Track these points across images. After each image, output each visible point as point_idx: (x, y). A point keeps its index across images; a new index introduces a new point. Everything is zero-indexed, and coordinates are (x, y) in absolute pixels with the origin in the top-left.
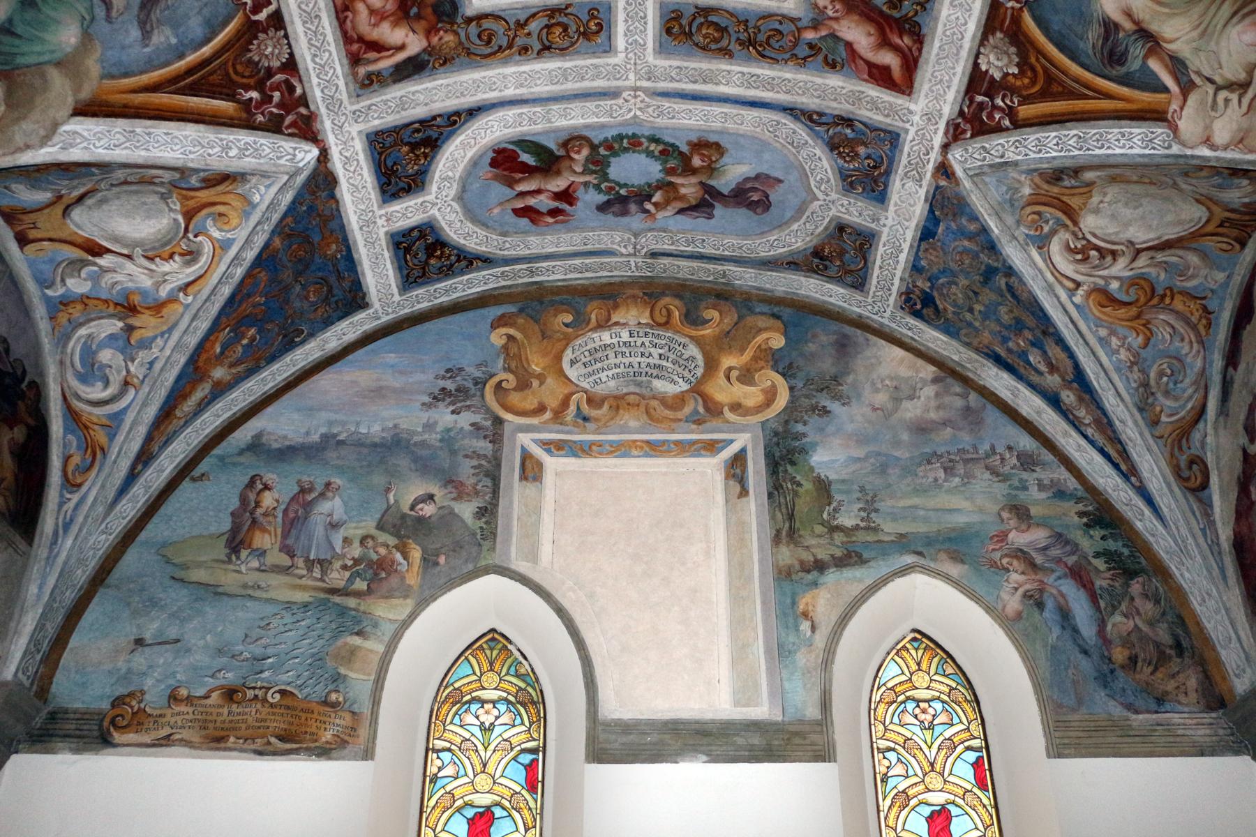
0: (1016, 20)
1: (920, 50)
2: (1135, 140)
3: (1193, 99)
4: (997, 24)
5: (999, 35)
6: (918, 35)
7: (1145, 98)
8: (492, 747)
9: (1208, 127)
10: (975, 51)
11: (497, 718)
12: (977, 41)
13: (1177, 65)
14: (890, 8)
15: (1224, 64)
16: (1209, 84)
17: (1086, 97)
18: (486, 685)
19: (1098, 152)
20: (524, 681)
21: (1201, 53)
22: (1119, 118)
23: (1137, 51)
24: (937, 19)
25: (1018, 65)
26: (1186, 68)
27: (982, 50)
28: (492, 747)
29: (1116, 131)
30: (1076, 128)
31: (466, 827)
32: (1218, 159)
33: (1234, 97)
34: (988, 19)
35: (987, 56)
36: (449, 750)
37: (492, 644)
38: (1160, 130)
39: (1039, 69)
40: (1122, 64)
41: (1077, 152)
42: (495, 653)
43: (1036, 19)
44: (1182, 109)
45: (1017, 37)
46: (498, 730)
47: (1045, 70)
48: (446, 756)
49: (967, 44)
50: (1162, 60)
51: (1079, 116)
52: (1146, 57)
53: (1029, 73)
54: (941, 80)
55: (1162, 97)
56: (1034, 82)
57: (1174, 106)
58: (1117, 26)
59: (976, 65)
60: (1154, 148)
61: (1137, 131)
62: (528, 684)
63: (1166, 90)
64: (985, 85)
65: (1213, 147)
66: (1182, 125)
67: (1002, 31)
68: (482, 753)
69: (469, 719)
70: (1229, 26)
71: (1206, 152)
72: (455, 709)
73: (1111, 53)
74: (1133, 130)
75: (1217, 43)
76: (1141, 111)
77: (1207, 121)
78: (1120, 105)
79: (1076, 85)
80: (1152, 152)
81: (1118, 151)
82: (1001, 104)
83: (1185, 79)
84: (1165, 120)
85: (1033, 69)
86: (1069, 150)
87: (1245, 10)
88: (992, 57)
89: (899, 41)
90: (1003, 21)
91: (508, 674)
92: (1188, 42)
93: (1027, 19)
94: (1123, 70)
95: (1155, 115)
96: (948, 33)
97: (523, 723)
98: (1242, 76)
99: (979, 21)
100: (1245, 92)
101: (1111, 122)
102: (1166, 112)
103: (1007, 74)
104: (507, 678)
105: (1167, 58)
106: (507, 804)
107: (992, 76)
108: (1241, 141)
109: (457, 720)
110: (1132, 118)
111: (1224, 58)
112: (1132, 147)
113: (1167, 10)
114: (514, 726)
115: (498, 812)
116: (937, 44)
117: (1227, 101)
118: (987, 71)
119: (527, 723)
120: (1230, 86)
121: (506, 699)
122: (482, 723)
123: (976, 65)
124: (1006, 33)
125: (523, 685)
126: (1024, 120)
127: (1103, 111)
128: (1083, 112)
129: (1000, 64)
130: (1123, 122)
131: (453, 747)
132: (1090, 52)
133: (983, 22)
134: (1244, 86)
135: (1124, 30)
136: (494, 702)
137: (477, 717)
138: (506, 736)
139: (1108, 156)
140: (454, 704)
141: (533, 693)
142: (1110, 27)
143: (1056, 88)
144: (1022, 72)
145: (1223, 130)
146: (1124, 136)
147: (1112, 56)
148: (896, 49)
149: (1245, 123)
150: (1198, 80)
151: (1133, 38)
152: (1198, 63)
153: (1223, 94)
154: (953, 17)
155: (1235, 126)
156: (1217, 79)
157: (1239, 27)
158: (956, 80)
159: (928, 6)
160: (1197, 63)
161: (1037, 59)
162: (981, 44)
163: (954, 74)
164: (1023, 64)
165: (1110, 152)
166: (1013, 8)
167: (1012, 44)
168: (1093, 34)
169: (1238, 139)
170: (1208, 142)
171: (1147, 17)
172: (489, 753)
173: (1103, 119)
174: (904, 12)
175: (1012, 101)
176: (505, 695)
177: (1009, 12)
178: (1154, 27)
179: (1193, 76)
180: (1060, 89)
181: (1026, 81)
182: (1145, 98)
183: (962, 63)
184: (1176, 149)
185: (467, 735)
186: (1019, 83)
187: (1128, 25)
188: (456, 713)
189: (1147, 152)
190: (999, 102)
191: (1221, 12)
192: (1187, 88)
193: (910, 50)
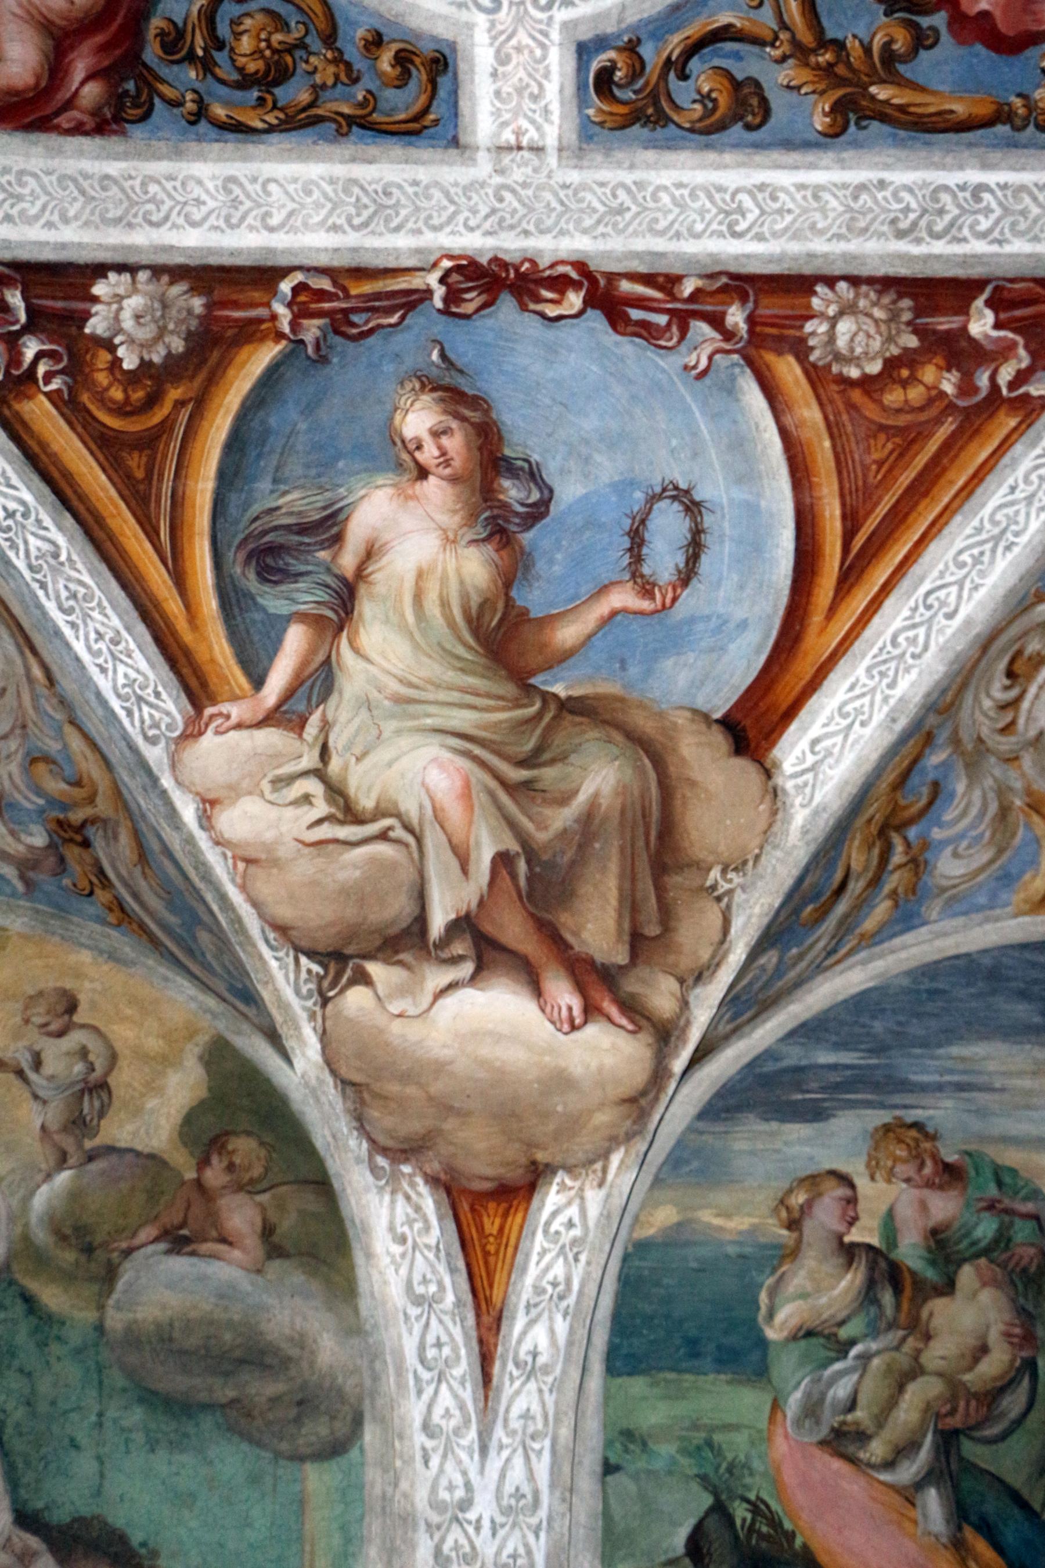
0: (252, 332)
1: (78, 130)
2: (121, 669)
3: (271, 737)
4: (220, 293)
5: (197, 303)
6: (118, 119)
7: (217, 648)
9: (235, 792)
10: (132, 259)
12: (162, 259)
13: (318, 681)
14: (162, 34)
15: (367, 762)
16: (316, 752)
17: (151, 533)
19: (51, 607)
21: (364, 714)
22: (145, 616)
23: (307, 596)
24: (178, 154)
25: (145, 365)
26: (323, 699)
27: (143, 276)
29: (116, 622)
30: (71, 540)
32: (190, 840)
33: (321, 808)
34: (222, 269)
35: (135, 290)
38: (172, 707)
39: (158, 416)
40: (263, 578)
41: (20, 564)
43: (270, 380)
44: (239, 726)
45: (211, 347)
47: (166, 427)
49: (142, 240)
50: (312, 651)
51: (100, 535)
52: (302, 617)
53: (138, 395)
54: (19, 198)
55: (240, 679)
56: (122, 410)
57: (236, 711)
58: (338, 539)
59: (100, 270)
60: (130, 713)
61: (143, 665)
63: (258, 682)
64: (60, 304)
65: (206, 820)
66: (208, 740)
67: (209, 306)
70: (439, 738)
71: (188, 812)
73: (273, 550)
74: (137, 655)
75: (398, 732)
76: (187, 653)
77: (245, 784)
78: (174, 606)
79: (166, 503)
80: (122, 714)
81: (79, 647)
82: (29, 354)
83: (301, 707)
84: (198, 706)
85: (153, 400)
86: (14, 546)
87: (477, 751)
88: (134, 303)
89: (79, 69)
90: (236, 305)
92: (372, 681)
93: (261, 358)
94: (251, 582)
95: (193, 683)
96: (153, 188)
98: (367, 803)
99: (210, 251)
100: (342, 823)
101: (125, 603)
102: (213, 701)
103: (112, 348)
105: (320, 657)
107: (87, 315)
108: (249, 861)
110: (159, 640)
111: (381, 755)
112: (103, 670)
113: (410, 618)
116: (114, 168)
117: (306, 799)
118: (95, 299)
120: (336, 791)
123: (100, 270)
124: (207, 319)
126: (17, 415)
127: (140, 578)
128: (111, 537)
129: (128, 323)
130: (141, 628)
132: (256, 509)
133: (213, 261)
134: (348, 812)
135: (334, 557)
139: (58, 633)
142: (329, 527)
143: (136, 463)
144: (132, 378)
145: (247, 819)
146: (115, 642)
147: (270, 556)
148: (56, 67)
149: (286, 850)
150: (312, 729)
151: (329, 580)
152: (344, 715)
153: (313, 786)
154: (197, 191)
155: (269, 836)
156: (335, 765)
157: (447, 755)
158: (36, 233)
159: (203, 126)
160: (343, 716)
161: (180, 404)
162: (157, 271)
163: (50, 225)
164: (153, 378)
165: (68, 632)
166: (274, 317)
167: (189, 337)
168: (297, 502)
169: (252, 854)
170: (209, 806)
171: (380, 589)
173: (124, 586)
174: (164, 71)
175: (48, 377)
177: (261, 312)
178: (367, 608)
179: (315, 719)
180: (140, 474)
181: (117, 394)
182: (217, 648)
183: (87, 237)
184: (155, 755)
186: (102, 378)
187: (348, 561)
189: (115, 704)
190: (31, 348)
191: (456, 712)
192: (286, 716)
193: (70, 104)
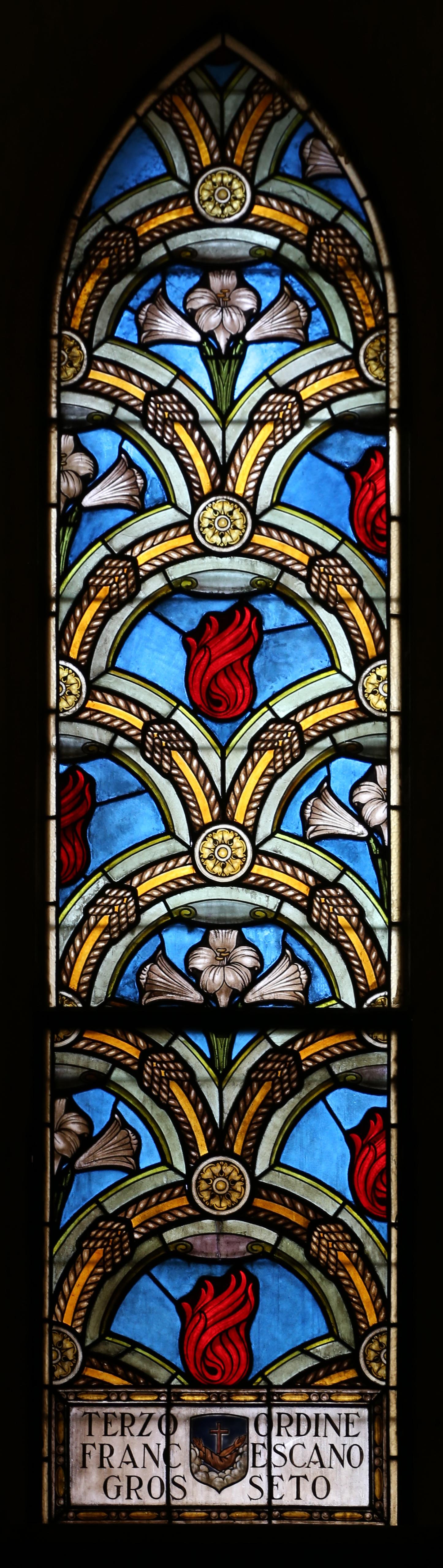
8: (242, 411)
11: (252, 318)
18: (210, 210)
20: (332, 198)
28: (242, 411)
31: (181, 658)
36: (109, 423)
37: (221, 74)
42: (232, 103)
46: (255, 361)
48: (105, 443)
62: (344, 208)
68: (214, 432)
69: (170, 324)
72: (117, 290)
91: (277, 173)
97: (333, 336)
104: (277, 186)
106: (299, 588)
109: (126, 328)
114: (305, 344)
115: (273, 614)
119: (346, 335)
121: (274, 256)
122: (208, 336)
125: (326, 210)
131: (123, 414)
136: (241, 267)
137: (190, 317)
138: (283, 376)
140: (114, 275)
141: (362, 238)
172: (234, 432)
176: (272, 242)
185: (163, 376)
188: (122, 305)
